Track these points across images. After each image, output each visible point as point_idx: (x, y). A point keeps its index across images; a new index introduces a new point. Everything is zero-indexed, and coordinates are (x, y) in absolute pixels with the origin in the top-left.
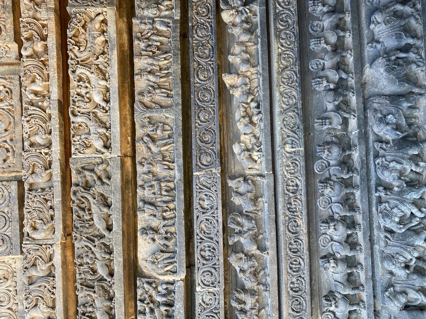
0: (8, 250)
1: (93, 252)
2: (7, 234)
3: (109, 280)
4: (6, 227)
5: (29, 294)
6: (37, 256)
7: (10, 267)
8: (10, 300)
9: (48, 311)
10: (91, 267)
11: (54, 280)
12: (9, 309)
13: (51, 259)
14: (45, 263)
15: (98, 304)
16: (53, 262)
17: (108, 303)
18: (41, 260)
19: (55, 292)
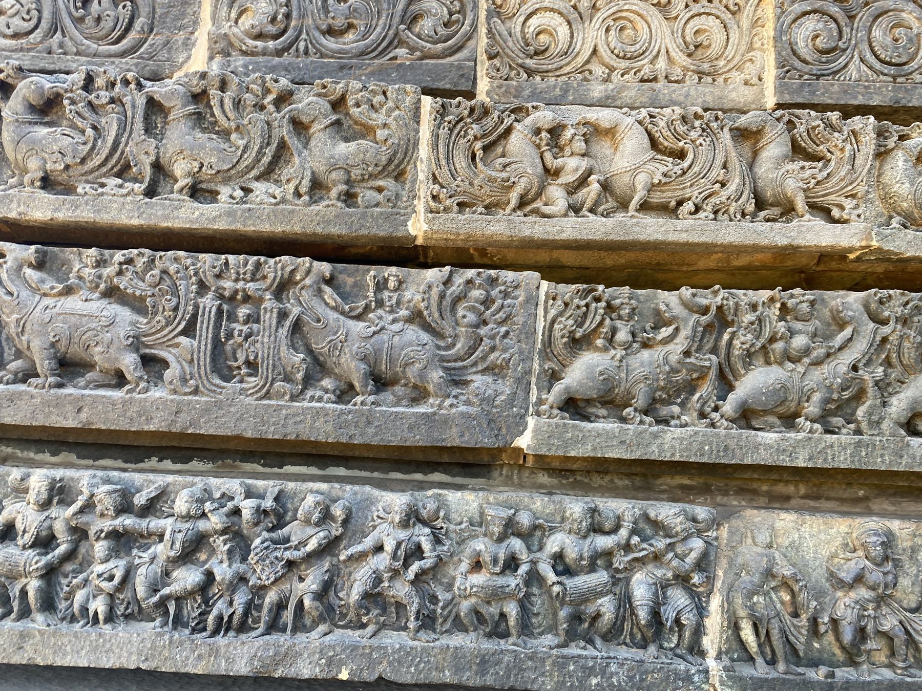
0: (798, 64)
1: (828, 355)
2: (852, 66)
3: (729, 406)
4: (878, 65)
5: (703, 130)
6: (833, 163)
7: (731, 65)
8: (624, 58)
9: (640, 186)
10: (779, 346)
11: (744, 215)
12: (595, 51)
13: (814, 207)
14: (805, 190)
15: (642, 364)
16: (807, 216)
17: (640, 401)
18: (819, 178)
19: (702, 215)
